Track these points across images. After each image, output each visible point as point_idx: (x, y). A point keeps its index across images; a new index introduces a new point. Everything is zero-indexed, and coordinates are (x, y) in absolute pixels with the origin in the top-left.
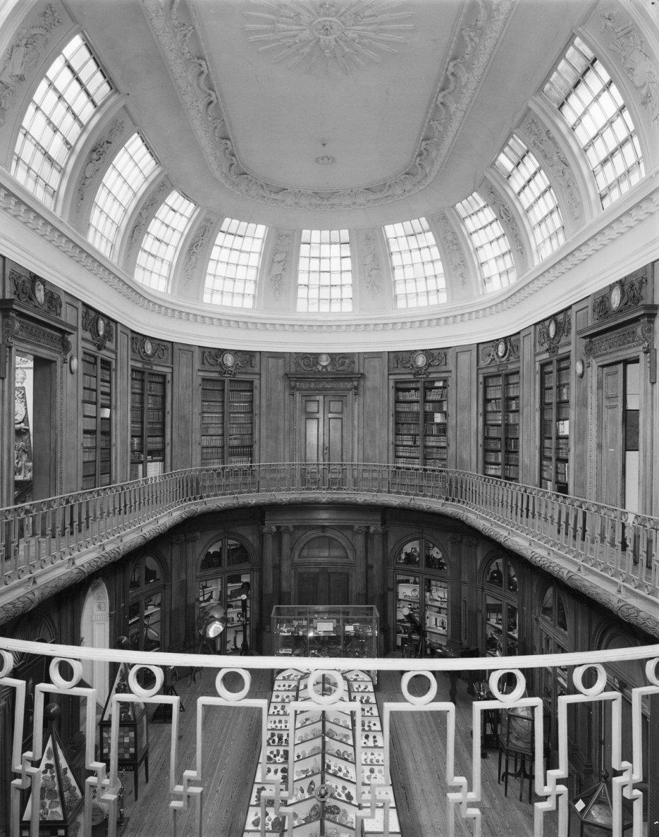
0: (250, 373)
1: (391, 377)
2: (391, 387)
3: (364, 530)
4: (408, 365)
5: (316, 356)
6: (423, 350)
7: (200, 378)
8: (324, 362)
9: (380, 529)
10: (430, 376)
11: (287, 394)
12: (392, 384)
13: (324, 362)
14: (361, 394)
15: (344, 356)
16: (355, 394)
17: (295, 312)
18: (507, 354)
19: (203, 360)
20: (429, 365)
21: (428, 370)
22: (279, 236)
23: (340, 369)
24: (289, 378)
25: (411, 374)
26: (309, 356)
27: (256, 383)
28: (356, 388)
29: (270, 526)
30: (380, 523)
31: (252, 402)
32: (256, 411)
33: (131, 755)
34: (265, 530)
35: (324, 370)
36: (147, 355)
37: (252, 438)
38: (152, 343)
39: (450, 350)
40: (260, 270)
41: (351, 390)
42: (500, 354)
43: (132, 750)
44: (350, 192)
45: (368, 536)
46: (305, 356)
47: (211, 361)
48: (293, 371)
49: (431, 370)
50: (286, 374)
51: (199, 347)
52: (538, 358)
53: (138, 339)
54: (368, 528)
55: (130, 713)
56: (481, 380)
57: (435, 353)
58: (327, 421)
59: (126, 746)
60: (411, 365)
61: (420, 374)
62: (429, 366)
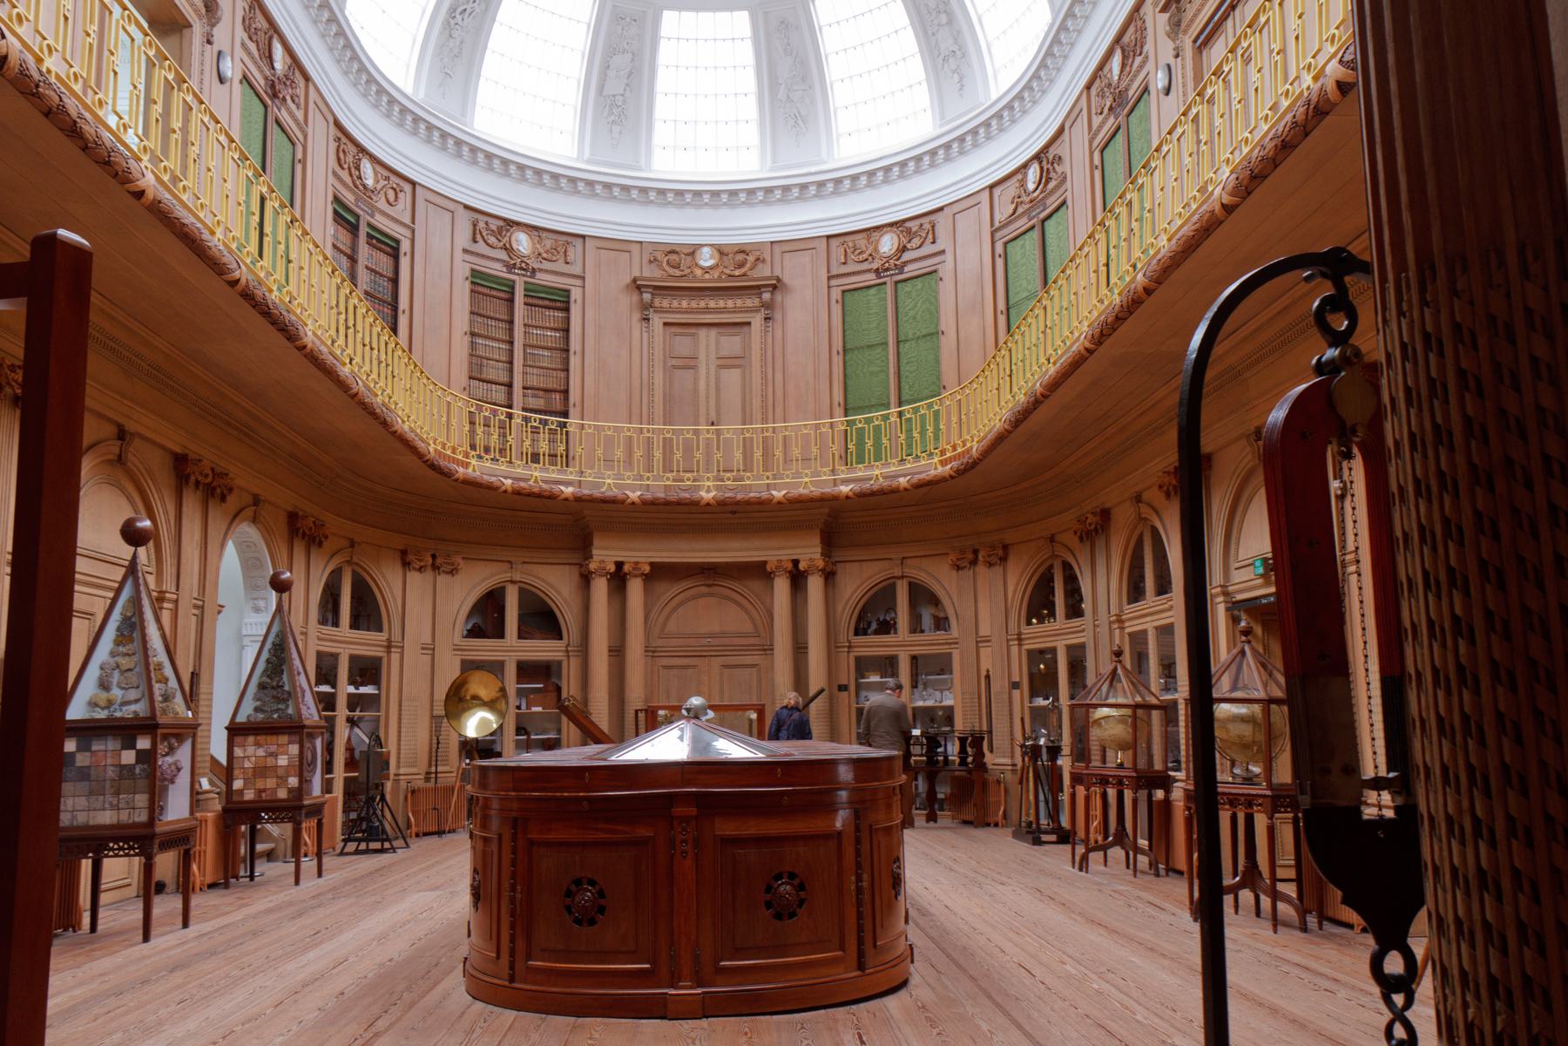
0: (562, 274)
1: (834, 282)
2: (833, 302)
3: (790, 566)
4: (865, 256)
5: (693, 251)
6: (891, 225)
7: (468, 266)
8: (706, 259)
9: (821, 564)
10: (906, 269)
11: (637, 316)
12: (836, 294)
13: (706, 259)
14: (778, 315)
15: (742, 250)
17: (651, 171)
18: (1043, 181)
19: (474, 234)
20: (903, 249)
21: (902, 260)
23: (737, 273)
24: (639, 288)
25: (869, 271)
26: (678, 250)
27: (576, 294)
28: (768, 306)
29: (605, 554)
31: (567, 330)
32: (575, 345)
33: (290, 791)
34: (593, 566)
35: (707, 276)
36: (364, 186)
37: (566, 399)
38: (374, 169)
39: (938, 217)
41: (757, 311)
42: (1031, 186)
43: (293, 781)
45: (798, 579)
47: (492, 240)
48: (646, 274)
49: (907, 256)
50: (635, 280)
51: (467, 207)
53: (349, 148)
54: (796, 562)
55: (290, 711)
56: (999, 249)
57: (914, 225)
58: (713, 369)
59: (281, 772)
60: (871, 255)
61: (887, 270)
62: (904, 251)
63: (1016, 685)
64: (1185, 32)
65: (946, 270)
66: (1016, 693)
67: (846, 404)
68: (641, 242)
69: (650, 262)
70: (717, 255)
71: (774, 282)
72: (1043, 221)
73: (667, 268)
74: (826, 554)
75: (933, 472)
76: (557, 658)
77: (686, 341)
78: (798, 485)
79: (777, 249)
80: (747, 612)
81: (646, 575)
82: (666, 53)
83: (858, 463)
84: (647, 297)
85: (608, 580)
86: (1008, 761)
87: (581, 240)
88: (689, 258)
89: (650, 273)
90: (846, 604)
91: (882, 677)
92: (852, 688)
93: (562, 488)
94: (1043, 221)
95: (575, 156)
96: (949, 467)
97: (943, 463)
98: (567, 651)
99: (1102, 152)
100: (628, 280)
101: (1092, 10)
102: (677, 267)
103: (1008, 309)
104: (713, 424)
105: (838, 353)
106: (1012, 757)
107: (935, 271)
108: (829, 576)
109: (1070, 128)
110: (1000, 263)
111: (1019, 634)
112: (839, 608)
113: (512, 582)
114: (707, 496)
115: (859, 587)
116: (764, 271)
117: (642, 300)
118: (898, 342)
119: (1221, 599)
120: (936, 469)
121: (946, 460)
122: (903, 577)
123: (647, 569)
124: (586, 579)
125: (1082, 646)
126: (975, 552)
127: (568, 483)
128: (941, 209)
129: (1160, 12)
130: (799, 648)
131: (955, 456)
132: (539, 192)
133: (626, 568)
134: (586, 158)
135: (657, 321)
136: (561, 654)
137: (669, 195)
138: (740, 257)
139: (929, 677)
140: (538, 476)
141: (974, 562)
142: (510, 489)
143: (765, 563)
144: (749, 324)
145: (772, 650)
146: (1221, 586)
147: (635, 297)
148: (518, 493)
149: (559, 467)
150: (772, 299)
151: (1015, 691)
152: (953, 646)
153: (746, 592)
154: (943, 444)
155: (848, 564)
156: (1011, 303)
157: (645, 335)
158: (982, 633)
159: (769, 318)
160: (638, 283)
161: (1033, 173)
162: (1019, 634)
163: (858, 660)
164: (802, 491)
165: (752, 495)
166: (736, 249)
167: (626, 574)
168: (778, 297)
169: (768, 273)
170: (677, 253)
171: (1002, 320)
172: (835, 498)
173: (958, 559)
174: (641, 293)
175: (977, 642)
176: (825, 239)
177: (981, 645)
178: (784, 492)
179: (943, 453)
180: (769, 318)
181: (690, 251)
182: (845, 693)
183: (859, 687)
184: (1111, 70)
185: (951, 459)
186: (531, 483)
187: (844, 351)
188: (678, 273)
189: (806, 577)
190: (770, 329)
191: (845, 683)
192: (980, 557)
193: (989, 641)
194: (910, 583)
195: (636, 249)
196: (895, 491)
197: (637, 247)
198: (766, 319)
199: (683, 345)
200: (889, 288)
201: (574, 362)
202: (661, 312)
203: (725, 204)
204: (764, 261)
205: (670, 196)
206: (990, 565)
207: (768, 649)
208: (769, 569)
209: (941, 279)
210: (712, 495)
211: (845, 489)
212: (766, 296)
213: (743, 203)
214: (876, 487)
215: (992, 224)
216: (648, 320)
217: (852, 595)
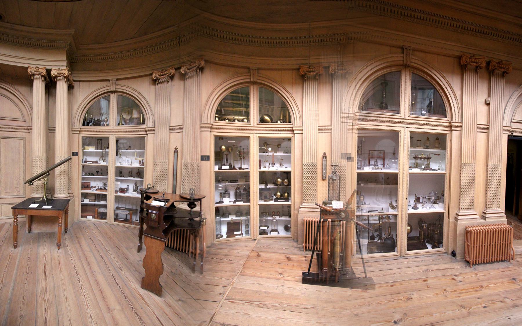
80: (17, 105)
90: (80, 106)
91: (95, 149)
92: (80, 154)
112: (75, 107)
115: (87, 97)
130: (50, 130)
139: (123, 151)
145: (32, 129)
153: (17, 93)
155: (81, 83)
163: (84, 139)
182: (77, 157)
183: (84, 154)
207: (29, 129)
217: (83, 101)
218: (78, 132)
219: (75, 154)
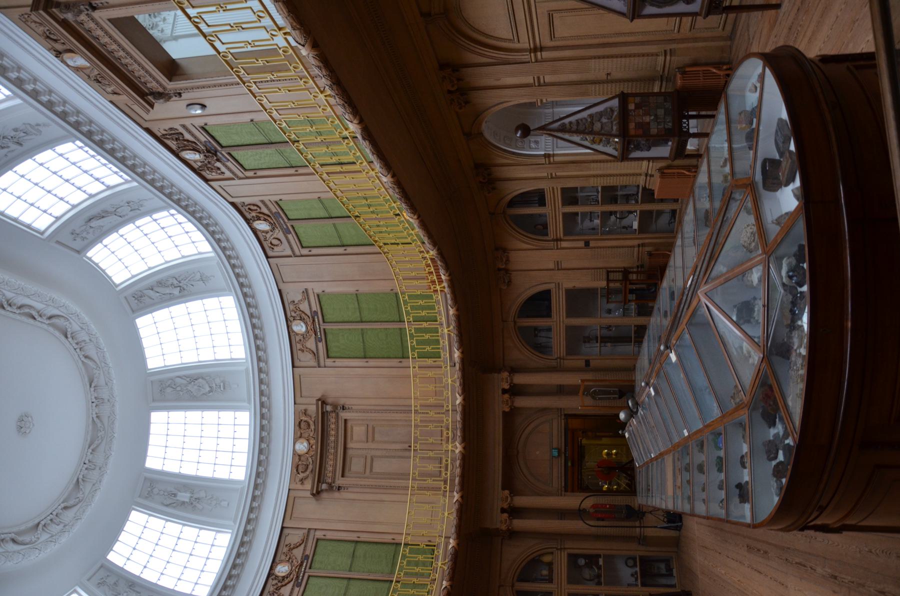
1: (322, 364)
3: (507, 396)
9: (505, 374)
11: (336, 495)
12: (329, 362)
13: (302, 447)
14: (342, 402)
15: (299, 424)
16: (343, 408)
22: (149, 495)
23: (312, 427)
27: (319, 534)
28: (335, 406)
30: (496, 374)
34: (504, 527)
35: (314, 447)
40: (186, 520)
44: (94, 405)
45: (515, 391)
46: (296, 468)
50: (313, 495)
52: (240, 175)
54: (504, 391)
56: (305, 252)
58: (373, 446)
63: (587, 244)
64: (164, 88)
65: (318, 288)
66: (592, 244)
67: (401, 358)
68: (289, 489)
69: (302, 484)
70: (301, 440)
71: (320, 402)
72: (289, 219)
73: (308, 473)
74: (499, 371)
75: (447, 290)
76: (566, 558)
77: (354, 461)
78: (453, 387)
79: (299, 400)
81: (510, 493)
82: (172, 467)
83: (437, 332)
84: (324, 486)
85: (514, 518)
86: (636, 249)
87: (286, 531)
88: (302, 458)
89: (308, 485)
93: (450, 547)
94: (289, 219)
95: (231, 531)
96: (443, 277)
97: (441, 282)
98: (561, 549)
99: (245, 170)
100: (313, 501)
101: (158, 173)
102: (307, 466)
103: (343, 246)
104: (410, 446)
105: (367, 362)
106: (634, 247)
107: (318, 295)
108: (513, 370)
109: (232, 197)
110: (315, 251)
111: (553, 240)
113: (513, 586)
114: (459, 448)
116: (312, 409)
117: (326, 490)
118: (362, 322)
119: (539, 54)
120: (444, 287)
121: (438, 282)
122: (515, 322)
123: (507, 492)
124: (512, 534)
125: (564, 190)
126: (499, 270)
127: (447, 544)
128: (280, 291)
129: (153, 108)
131: (436, 272)
132: (251, 555)
133: (505, 506)
134: (233, 524)
135: (340, 481)
136: (563, 553)
137: (260, 470)
138: (303, 424)
140: (442, 564)
141: (507, 271)
142: (448, 583)
143: (504, 412)
144: (346, 421)
145: (561, 409)
146: (530, 53)
147: (324, 495)
148: (452, 578)
149: (435, 548)
150: (331, 405)
151: (591, 245)
152: (561, 287)
154: (429, 292)
156: (340, 244)
157: (350, 489)
158: (551, 266)
159: (343, 407)
160: (315, 492)
161: (262, 226)
162: (553, 240)
164: (458, 384)
165: (459, 419)
166: (297, 428)
167: (510, 506)
168: (330, 401)
169: (315, 406)
170: (298, 466)
171: (350, 250)
172: (463, 360)
173: (504, 282)
174: (322, 490)
175: (558, 269)
176: (294, 369)
177: (560, 267)
178: (457, 395)
179: (433, 282)
180: (343, 407)
181: (297, 458)
184: (195, 161)
185: (439, 276)
186: (446, 568)
187: (365, 358)
188: (310, 467)
189: (515, 384)
190: (350, 407)
191: (584, 361)
192: (503, 267)
193: (558, 262)
194: (519, 317)
195: (293, 493)
196: (458, 318)
197: (291, 491)
198: (343, 409)
199: (356, 465)
200: (328, 327)
201: (364, 537)
202: (334, 478)
203: (269, 434)
204: (306, 410)
205: (261, 469)
206: (508, 260)
208: (507, 410)
209: (323, 291)
210: (458, 445)
211: (457, 354)
212: (329, 408)
213: (269, 422)
214: (456, 332)
215: (291, 256)
216: (339, 487)
218: (562, 361)
219: (587, 363)
